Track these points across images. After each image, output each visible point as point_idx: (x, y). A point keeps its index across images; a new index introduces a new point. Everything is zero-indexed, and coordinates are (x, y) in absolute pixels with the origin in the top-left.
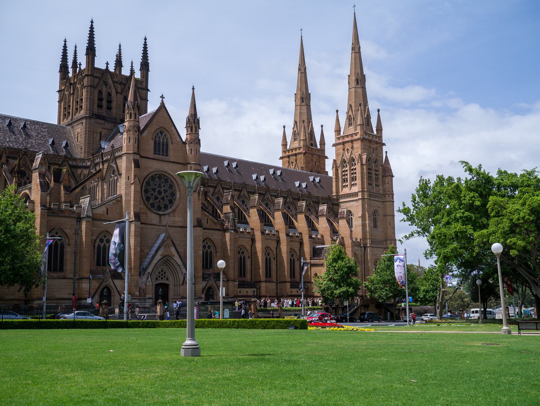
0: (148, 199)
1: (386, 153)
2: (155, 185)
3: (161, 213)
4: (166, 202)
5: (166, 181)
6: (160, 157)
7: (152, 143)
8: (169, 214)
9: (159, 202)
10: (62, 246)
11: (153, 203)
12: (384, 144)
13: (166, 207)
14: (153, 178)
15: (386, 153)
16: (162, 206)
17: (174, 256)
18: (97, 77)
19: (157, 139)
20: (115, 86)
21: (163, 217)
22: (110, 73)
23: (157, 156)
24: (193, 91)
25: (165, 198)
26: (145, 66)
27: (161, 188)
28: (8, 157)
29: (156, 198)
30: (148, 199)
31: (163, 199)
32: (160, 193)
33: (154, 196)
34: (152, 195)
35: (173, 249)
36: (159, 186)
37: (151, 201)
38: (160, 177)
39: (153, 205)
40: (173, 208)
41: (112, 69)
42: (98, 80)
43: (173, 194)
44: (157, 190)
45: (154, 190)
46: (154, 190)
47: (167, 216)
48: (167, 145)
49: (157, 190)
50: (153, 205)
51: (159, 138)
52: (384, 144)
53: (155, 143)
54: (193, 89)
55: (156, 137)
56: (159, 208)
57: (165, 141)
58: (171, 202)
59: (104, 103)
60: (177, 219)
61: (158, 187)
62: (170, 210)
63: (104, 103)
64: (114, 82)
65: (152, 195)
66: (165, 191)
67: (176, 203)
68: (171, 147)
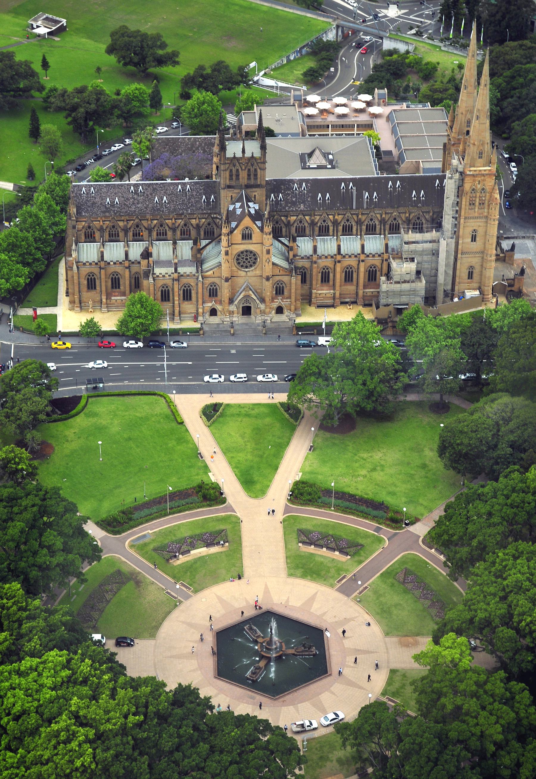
3: (247, 270)
4: (251, 263)
6: (247, 241)
7: (240, 236)
10: (190, 290)
13: (251, 266)
14: (242, 252)
22: (238, 159)
23: (244, 241)
28: (175, 219)
29: (244, 262)
32: (247, 259)
35: (251, 292)
39: (242, 266)
41: (239, 155)
45: (243, 258)
46: (243, 258)
56: (247, 267)
58: (254, 263)
59: (234, 178)
63: (234, 178)
64: (239, 163)
66: (250, 258)
67: (257, 264)
68: (253, 235)
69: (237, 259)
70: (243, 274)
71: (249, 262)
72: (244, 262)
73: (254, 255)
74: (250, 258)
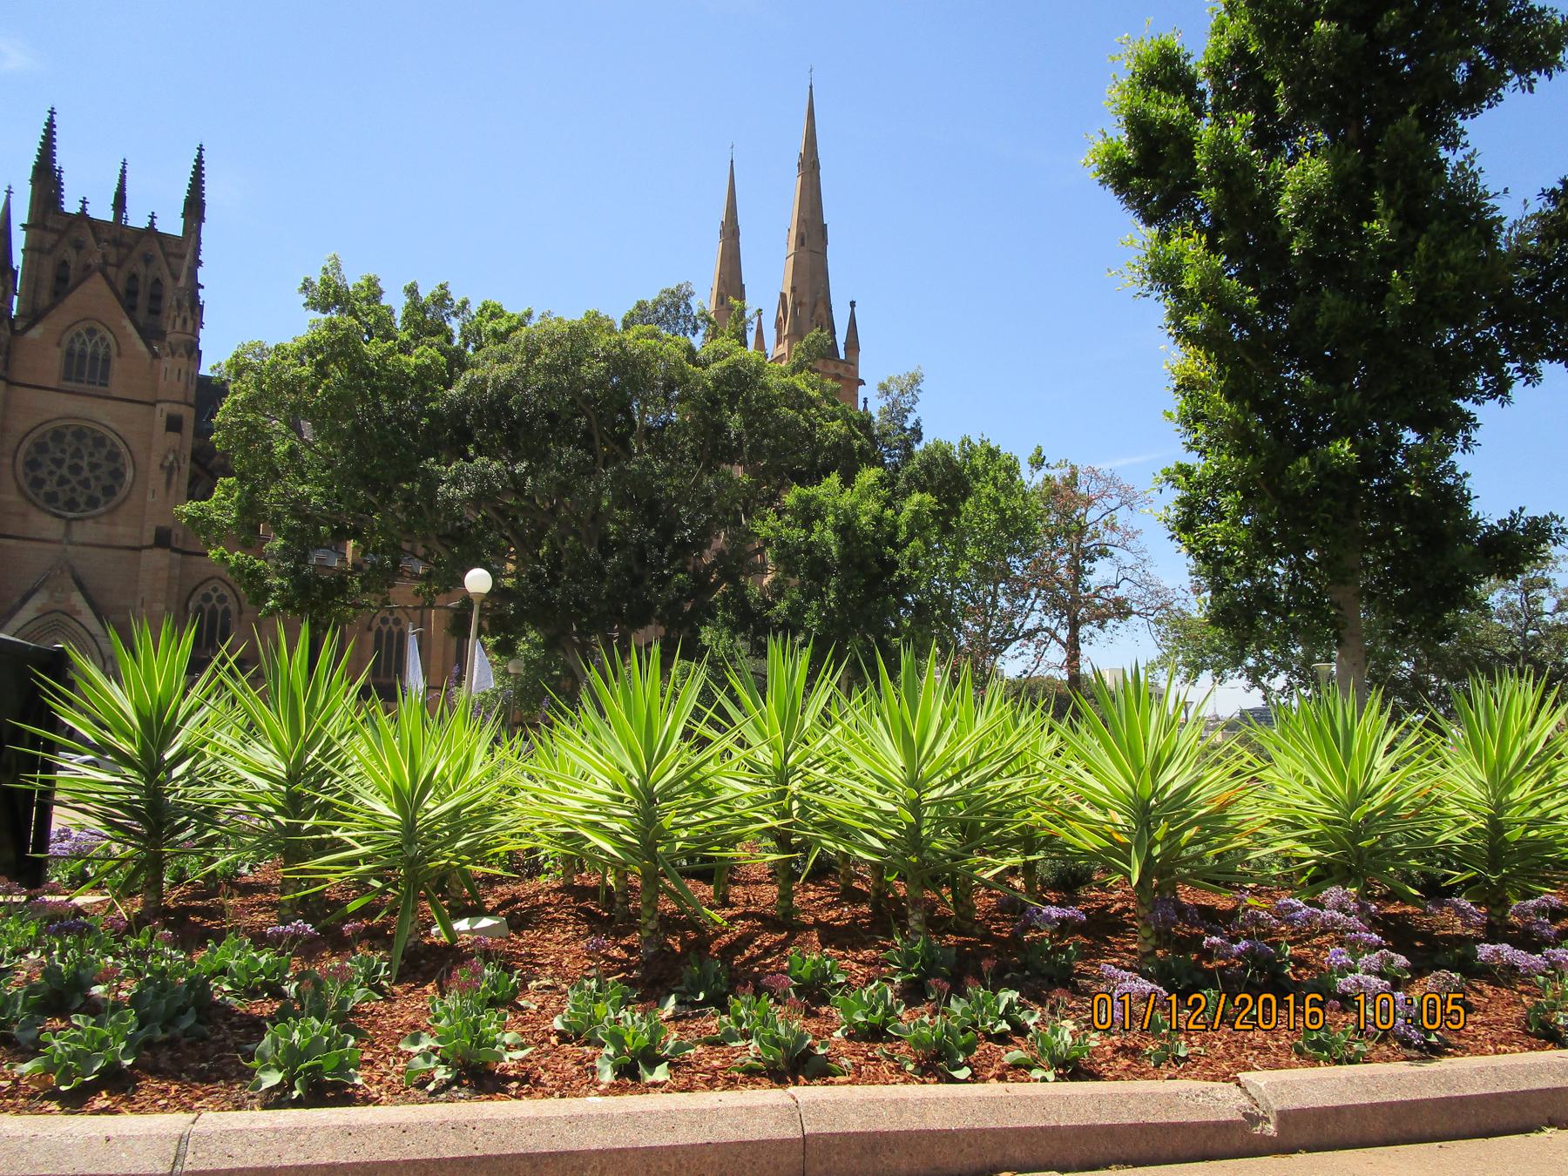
0: (37, 483)
1: (865, 401)
2: (63, 451)
3: (70, 515)
5: (100, 442)
7: (57, 355)
8: (93, 517)
9: (73, 490)
11: (55, 494)
12: (862, 382)
14: (58, 435)
15: (865, 401)
16: (82, 500)
17: (79, 613)
18: (52, 230)
19: (77, 347)
20: (169, 265)
21: (76, 526)
22: (96, 225)
23: (71, 385)
24: (8, 198)
25: (93, 483)
26: (195, 207)
27: (81, 458)
29: (62, 481)
30: (37, 483)
31: (85, 483)
32: (76, 469)
33: (56, 478)
34: (51, 473)
35: (77, 599)
36: (77, 454)
37: (47, 488)
38: (79, 434)
39: (51, 498)
40: (112, 504)
41: (102, 211)
42: (55, 237)
43: (118, 475)
44: (68, 462)
46: (59, 463)
47: (89, 523)
48: (107, 361)
49: (68, 462)
50: (51, 498)
51: (84, 343)
52: (862, 382)
53: (70, 354)
54: (9, 192)
55: (72, 341)
57: (101, 350)
58: (109, 491)
60: (121, 530)
61: (73, 456)
62: (102, 509)
65: (51, 473)
67: (121, 494)
68: (116, 364)
69: (32, 465)
70: (50, 526)
71: (85, 483)
72: (62, 481)
73: (114, 456)
74: (94, 467)
